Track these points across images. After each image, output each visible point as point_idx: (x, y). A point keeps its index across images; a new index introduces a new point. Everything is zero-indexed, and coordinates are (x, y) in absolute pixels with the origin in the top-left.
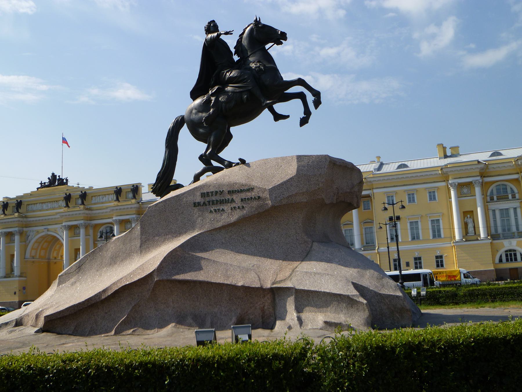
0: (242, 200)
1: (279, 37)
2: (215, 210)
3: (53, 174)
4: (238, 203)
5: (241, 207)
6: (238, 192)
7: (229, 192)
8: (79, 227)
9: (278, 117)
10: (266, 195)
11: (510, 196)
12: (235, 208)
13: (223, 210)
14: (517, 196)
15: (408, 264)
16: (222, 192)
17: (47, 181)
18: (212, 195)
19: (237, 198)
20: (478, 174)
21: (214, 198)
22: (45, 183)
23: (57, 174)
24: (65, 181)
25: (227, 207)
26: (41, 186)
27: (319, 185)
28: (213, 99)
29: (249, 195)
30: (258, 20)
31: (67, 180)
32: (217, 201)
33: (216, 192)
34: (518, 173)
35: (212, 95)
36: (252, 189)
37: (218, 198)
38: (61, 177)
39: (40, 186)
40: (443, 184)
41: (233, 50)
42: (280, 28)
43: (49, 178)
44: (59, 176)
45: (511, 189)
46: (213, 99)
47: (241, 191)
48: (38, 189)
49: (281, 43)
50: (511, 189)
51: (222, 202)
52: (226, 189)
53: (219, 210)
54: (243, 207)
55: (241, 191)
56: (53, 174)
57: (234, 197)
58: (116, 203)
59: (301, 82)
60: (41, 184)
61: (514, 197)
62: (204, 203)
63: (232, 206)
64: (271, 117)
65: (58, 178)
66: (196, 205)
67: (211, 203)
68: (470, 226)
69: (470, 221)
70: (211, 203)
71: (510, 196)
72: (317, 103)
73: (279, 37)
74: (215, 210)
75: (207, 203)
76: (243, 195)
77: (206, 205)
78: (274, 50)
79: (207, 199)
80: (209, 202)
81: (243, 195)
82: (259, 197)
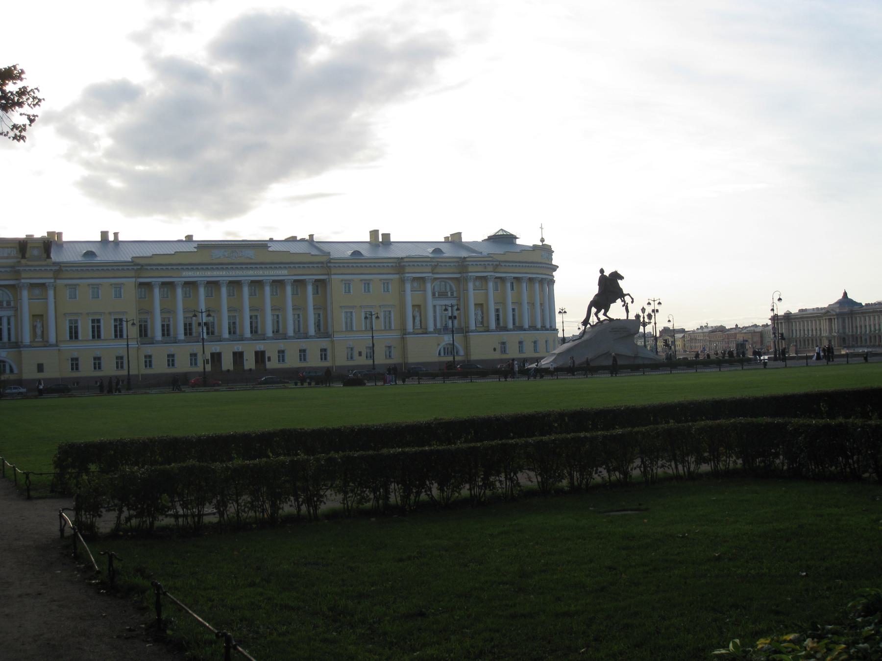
1: (622, 278)
11: (449, 294)
14: (455, 294)
15: (360, 354)
20: (430, 270)
34: (460, 273)
40: (397, 276)
42: (622, 274)
45: (450, 286)
50: (450, 286)
58: (23, 261)
59: (629, 295)
61: (452, 294)
68: (418, 319)
69: (418, 315)
71: (449, 294)
72: (632, 302)
73: (622, 278)
78: (619, 281)
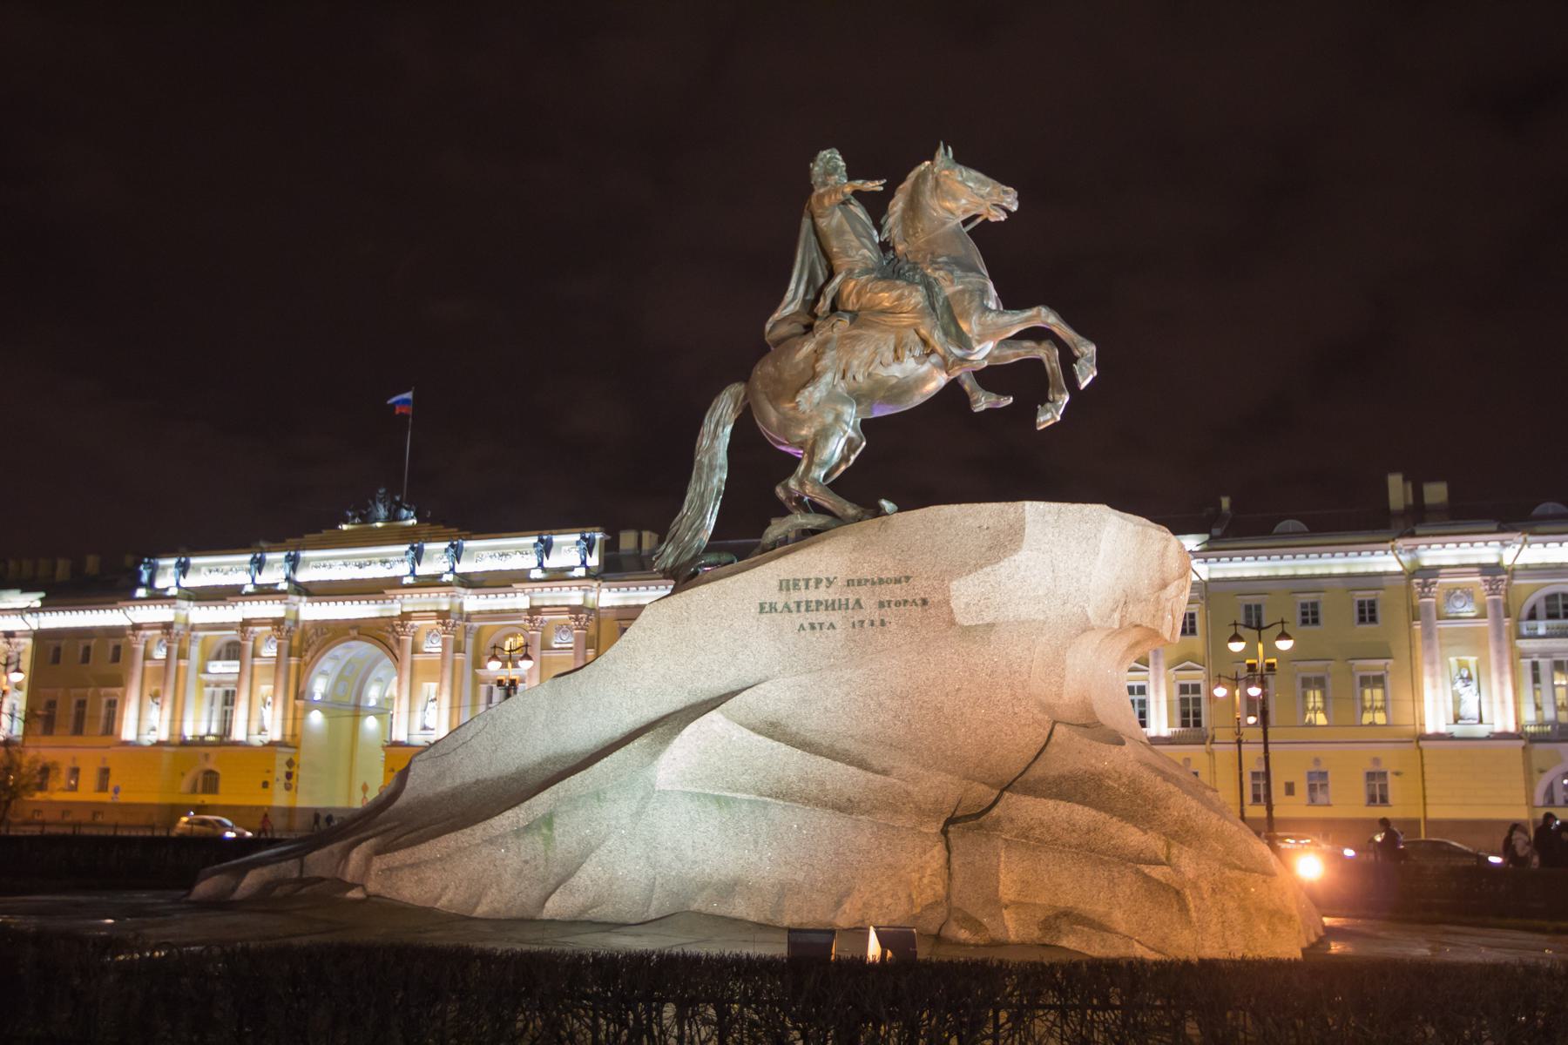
0: (881, 605)
2: (812, 627)
4: (870, 611)
5: (877, 623)
6: (873, 583)
7: (850, 583)
12: (862, 622)
13: (832, 626)
16: (830, 582)
18: (807, 587)
21: (813, 595)
27: (1078, 581)
29: (899, 592)
32: (819, 603)
33: (818, 581)
36: (908, 578)
37: (822, 594)
47: (881, 581)
51: (831, 606)
52: (842, 575)
53: (821, 625)
54: (883, 623)
55: (881, 581)
57: (863, 593)
62: (786, 606)
63: (856, 619)
67: (803, 608)
70: (803, 608)
74: (812, 627)
75: (793, 606)
76: (886, 593)
77: (790, 611)
79: (795, 596)
80: (798, 604)
81: (886, 593)
82: (925, 602)
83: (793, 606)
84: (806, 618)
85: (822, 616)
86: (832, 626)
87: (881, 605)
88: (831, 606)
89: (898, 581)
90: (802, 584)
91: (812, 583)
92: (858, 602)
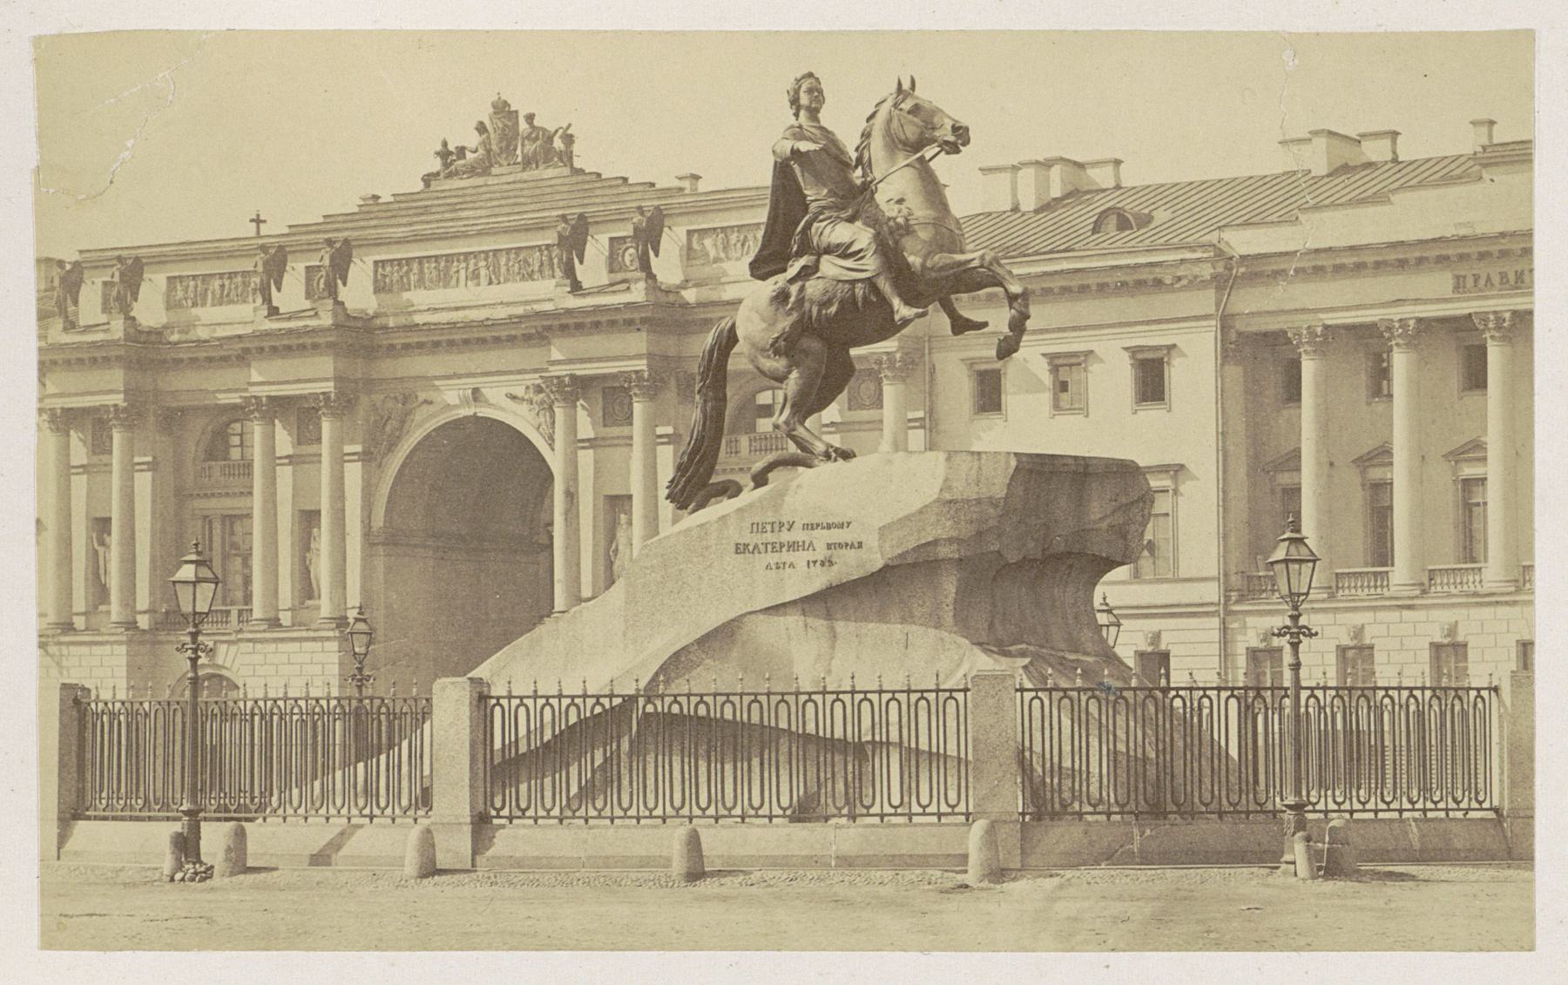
0: (829, 546)
3: (502, 109)
8: (626, 390)
9: (961, 325)
10: (872, 541)
17: (472, 140)
19: (821, 537)
22: (461, 151)
23: (521, 106)
24: (558, 144)
25: (800, 558)
26: (446, 165)
28: (794, 289)
30: (906, 85)
31: (569, 139)
35: (792, 281)
37: (786, 537)
38: (536, 123)
39: (436, 165)
41: (854, 155)
43: (481, 128)
44: (530, 118)
46: (794, 289)
48: (428, 179)
49: (958, 151)
51: (793, 546)
56: (502, 109)
60: (444, 154)
62: (756, 546)
64: (945, 321)
65: (523, 126)
66: (741, 549)
75: (762, 548)
82: (860, 545)
83: (762, 548)
84: (772, 558)
85: (786, 556)
86: (792, 565)
87: (829, 546)
88: (793, 546)
89: (841, 526)
90: (769, 528)
91: (776, 527)
92: (811, 544)
